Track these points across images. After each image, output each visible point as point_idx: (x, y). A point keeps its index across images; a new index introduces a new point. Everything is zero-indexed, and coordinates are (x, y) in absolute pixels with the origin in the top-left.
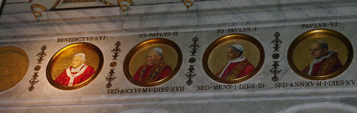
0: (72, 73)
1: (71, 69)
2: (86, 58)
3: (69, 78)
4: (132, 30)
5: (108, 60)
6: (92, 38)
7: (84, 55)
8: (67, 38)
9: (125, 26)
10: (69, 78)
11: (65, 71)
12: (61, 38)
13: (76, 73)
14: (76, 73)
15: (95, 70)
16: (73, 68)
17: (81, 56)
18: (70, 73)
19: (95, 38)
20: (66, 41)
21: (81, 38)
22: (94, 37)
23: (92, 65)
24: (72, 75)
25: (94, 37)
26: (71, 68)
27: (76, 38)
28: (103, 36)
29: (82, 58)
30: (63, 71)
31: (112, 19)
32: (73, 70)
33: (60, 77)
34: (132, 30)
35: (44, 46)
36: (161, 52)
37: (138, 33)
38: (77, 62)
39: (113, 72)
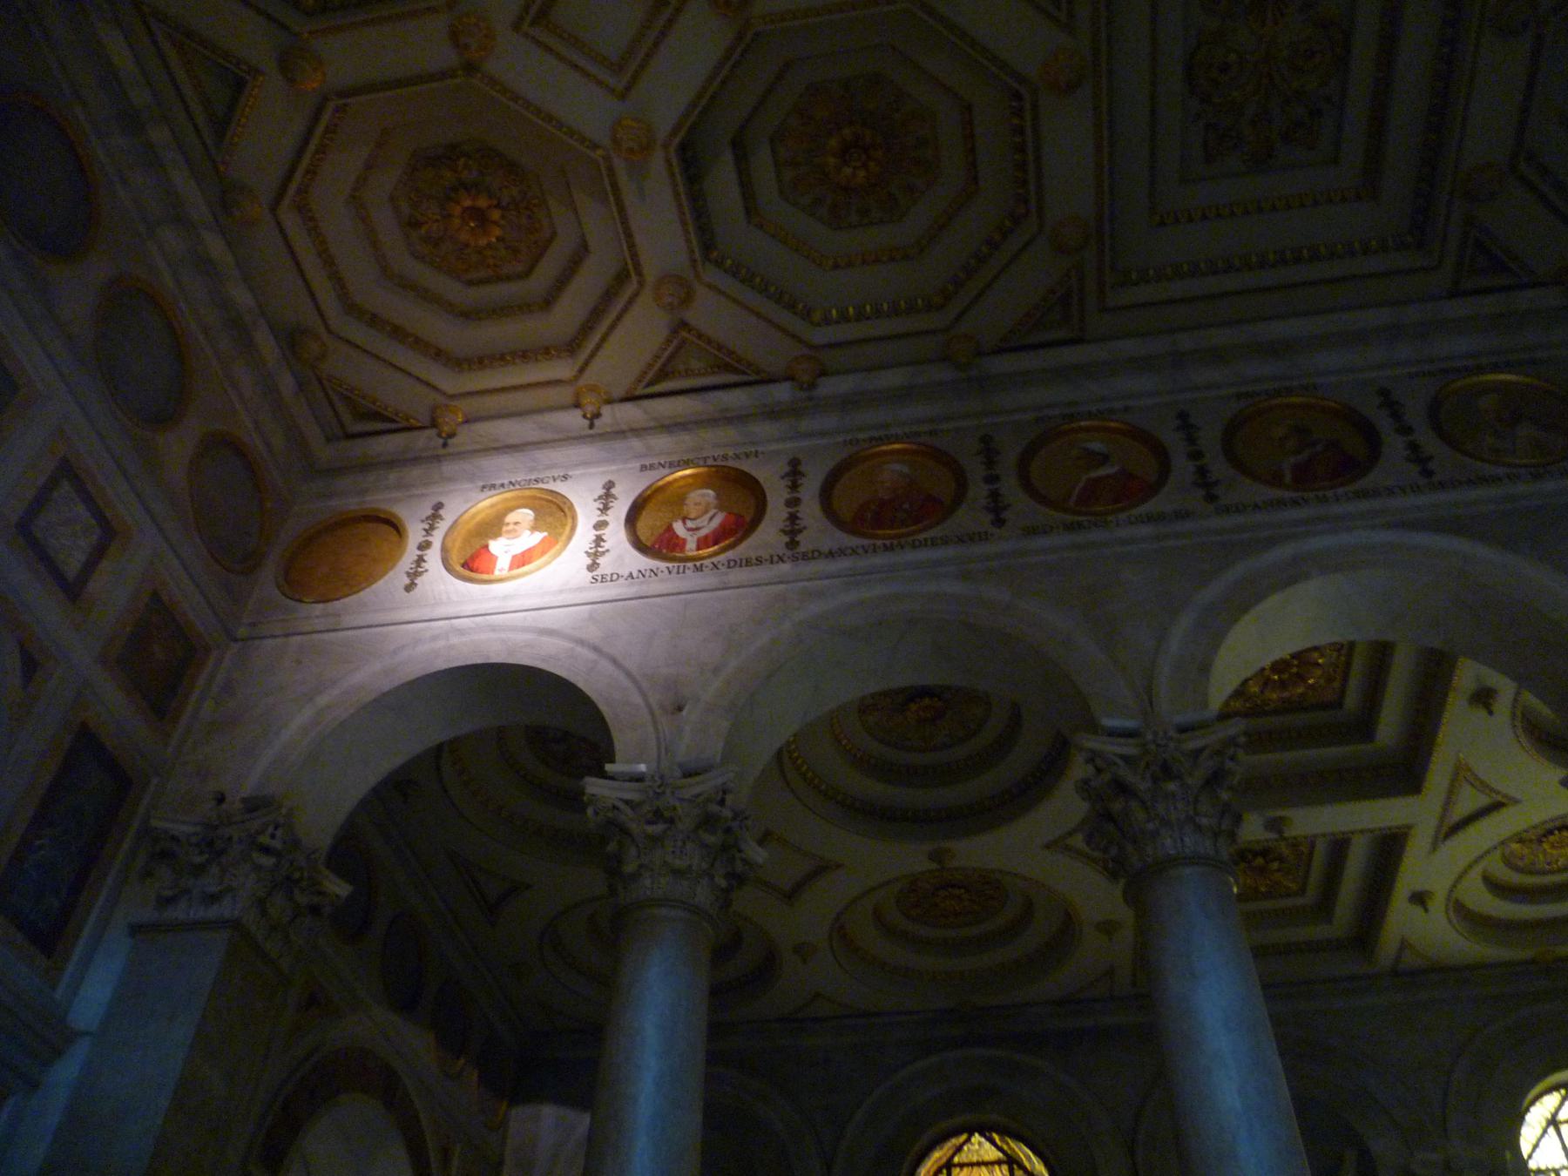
0: (689, 530)
1: (684, 523)
2: (718, 497)
3: (684, 541)
4: (823, 434)
5: (776, 496)
6: (725, 457)
7: (711, 492)
8: (662, 462)
9: (805, 425)
10: (684, 541)
11: (670, 529)
12: (648, 464)
13: (697, 529)
14: (697, 529)
15: (748, 519)
16: (690, 519)
17: (703, 495)
18: (685, 531)
19: (734, 456)
20: (661, 468)
21: (699, 458)
22: (731, 454)
23: (736, 511)
24: (691, 533)
25: (731, 454)
26: (684, 520)
27: (685, 459)
28: (753, 450)
29: (707, 498)
30: (664, 527)
31: (772, 413)
32: (690, 524)
33: (660, 539)
34: (823, 434)
35: (610, 482)
36: (906, 470)
37: (840, 439)
38: (697, 507)
39: (797, 518)
